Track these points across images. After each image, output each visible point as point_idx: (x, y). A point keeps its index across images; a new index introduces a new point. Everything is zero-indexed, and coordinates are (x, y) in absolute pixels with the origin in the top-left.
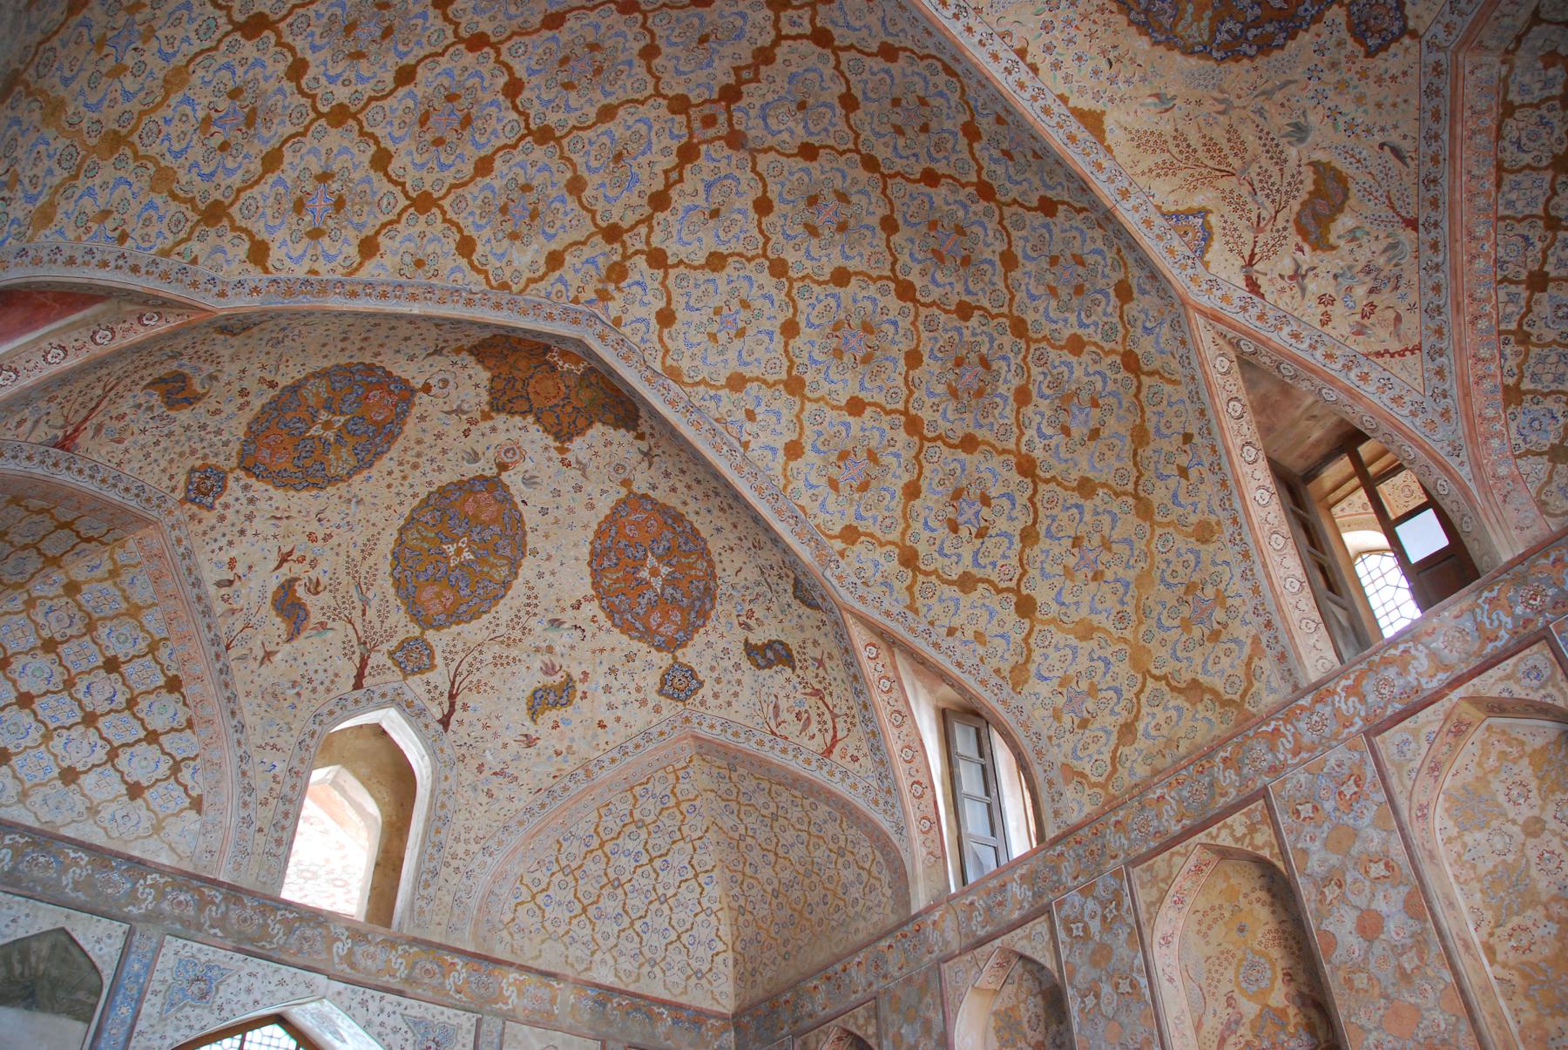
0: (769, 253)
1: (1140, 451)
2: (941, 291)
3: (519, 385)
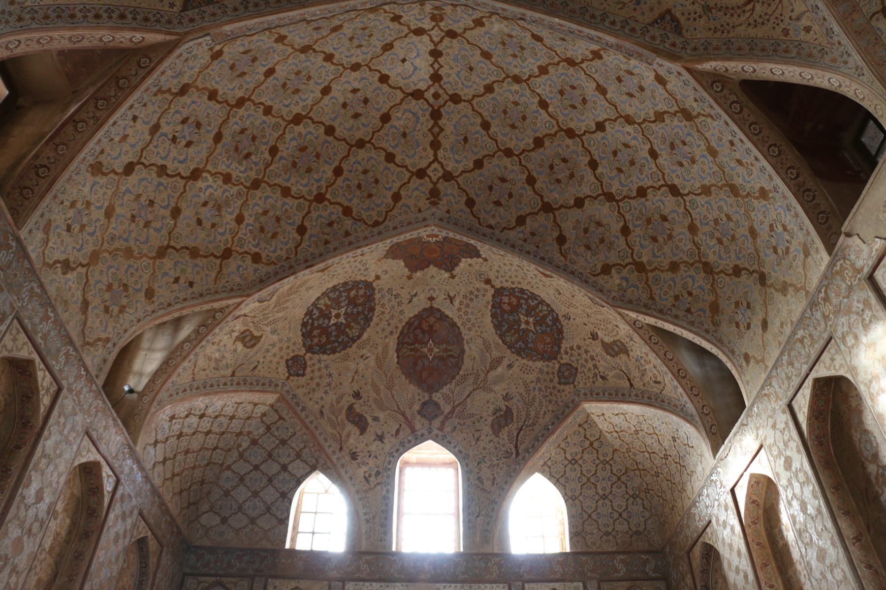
0: (365, 67)
1: (188, 252)
2: (288, 140)
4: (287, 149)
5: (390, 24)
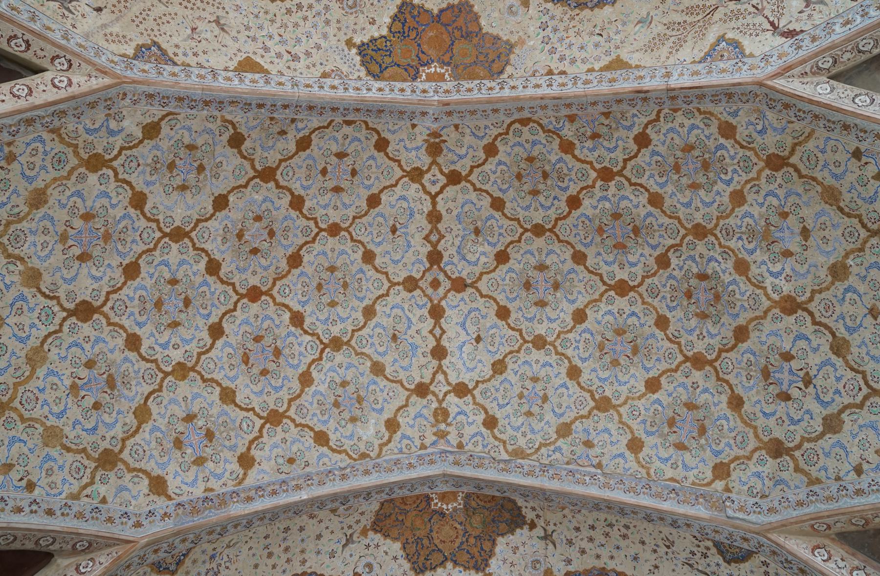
0: (527, 338)
1: (842, 204)
2: (641, 265)
3: (426, 542)
4: (642, 256)
5: (498, 415)
